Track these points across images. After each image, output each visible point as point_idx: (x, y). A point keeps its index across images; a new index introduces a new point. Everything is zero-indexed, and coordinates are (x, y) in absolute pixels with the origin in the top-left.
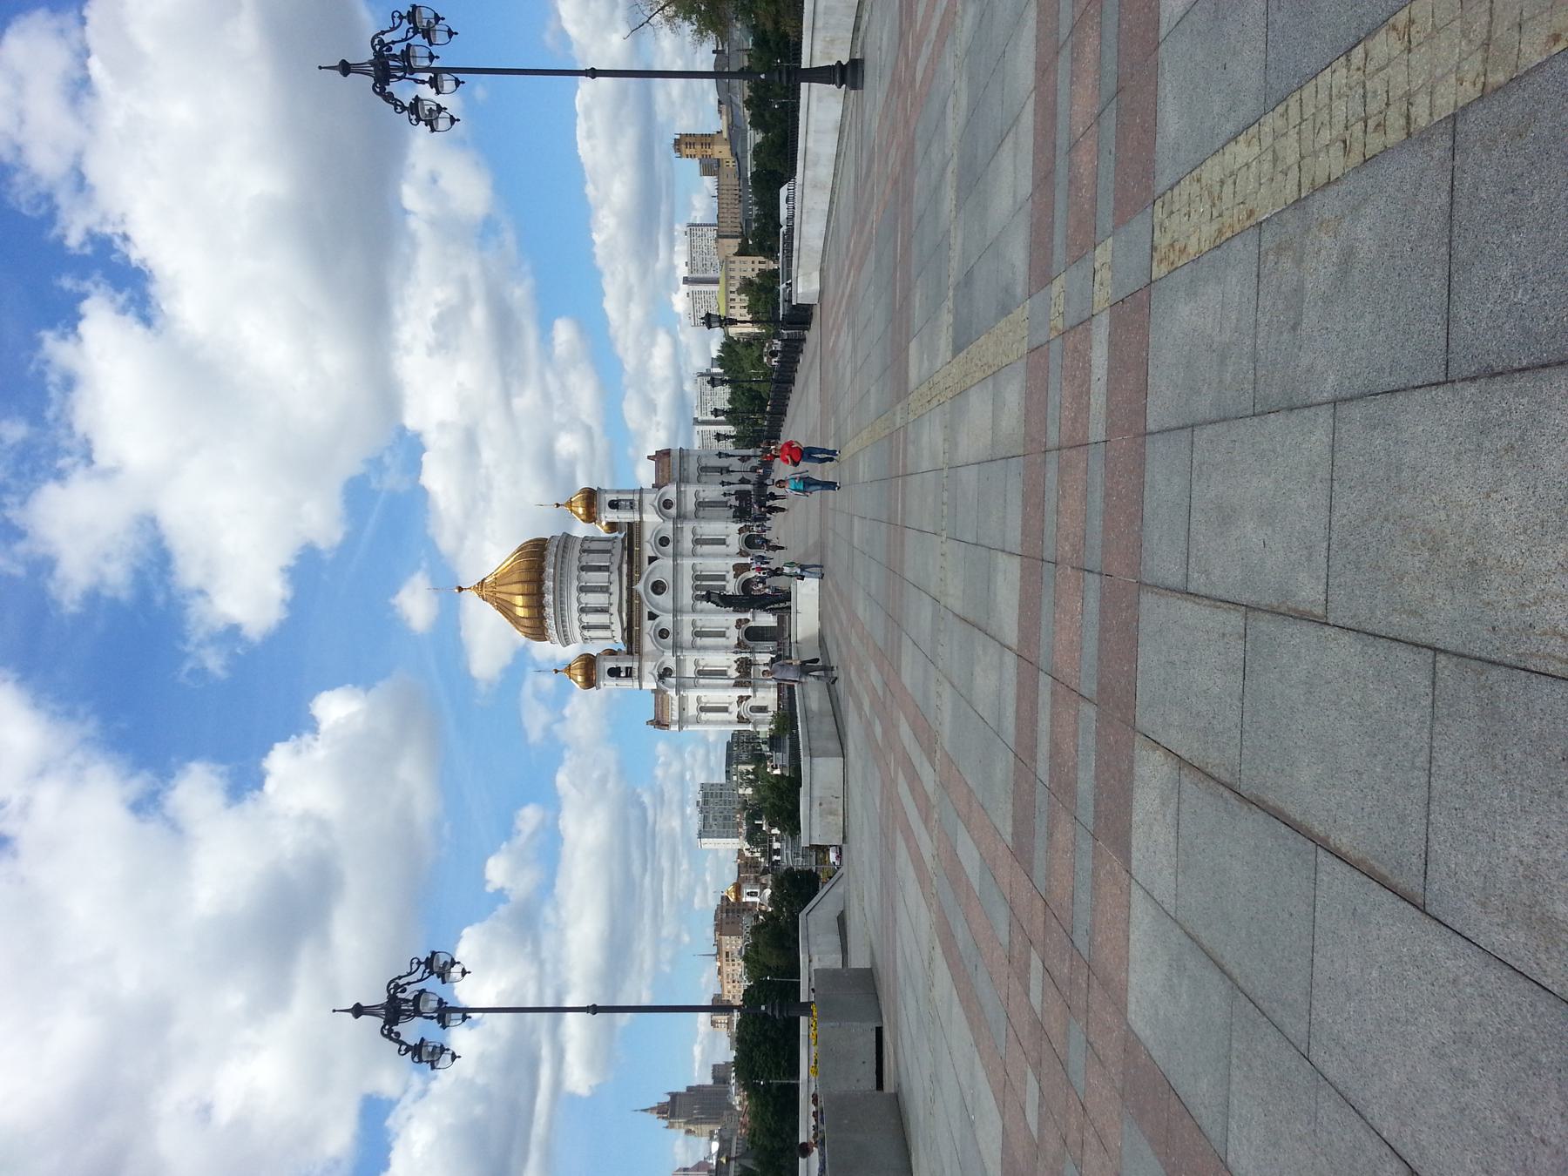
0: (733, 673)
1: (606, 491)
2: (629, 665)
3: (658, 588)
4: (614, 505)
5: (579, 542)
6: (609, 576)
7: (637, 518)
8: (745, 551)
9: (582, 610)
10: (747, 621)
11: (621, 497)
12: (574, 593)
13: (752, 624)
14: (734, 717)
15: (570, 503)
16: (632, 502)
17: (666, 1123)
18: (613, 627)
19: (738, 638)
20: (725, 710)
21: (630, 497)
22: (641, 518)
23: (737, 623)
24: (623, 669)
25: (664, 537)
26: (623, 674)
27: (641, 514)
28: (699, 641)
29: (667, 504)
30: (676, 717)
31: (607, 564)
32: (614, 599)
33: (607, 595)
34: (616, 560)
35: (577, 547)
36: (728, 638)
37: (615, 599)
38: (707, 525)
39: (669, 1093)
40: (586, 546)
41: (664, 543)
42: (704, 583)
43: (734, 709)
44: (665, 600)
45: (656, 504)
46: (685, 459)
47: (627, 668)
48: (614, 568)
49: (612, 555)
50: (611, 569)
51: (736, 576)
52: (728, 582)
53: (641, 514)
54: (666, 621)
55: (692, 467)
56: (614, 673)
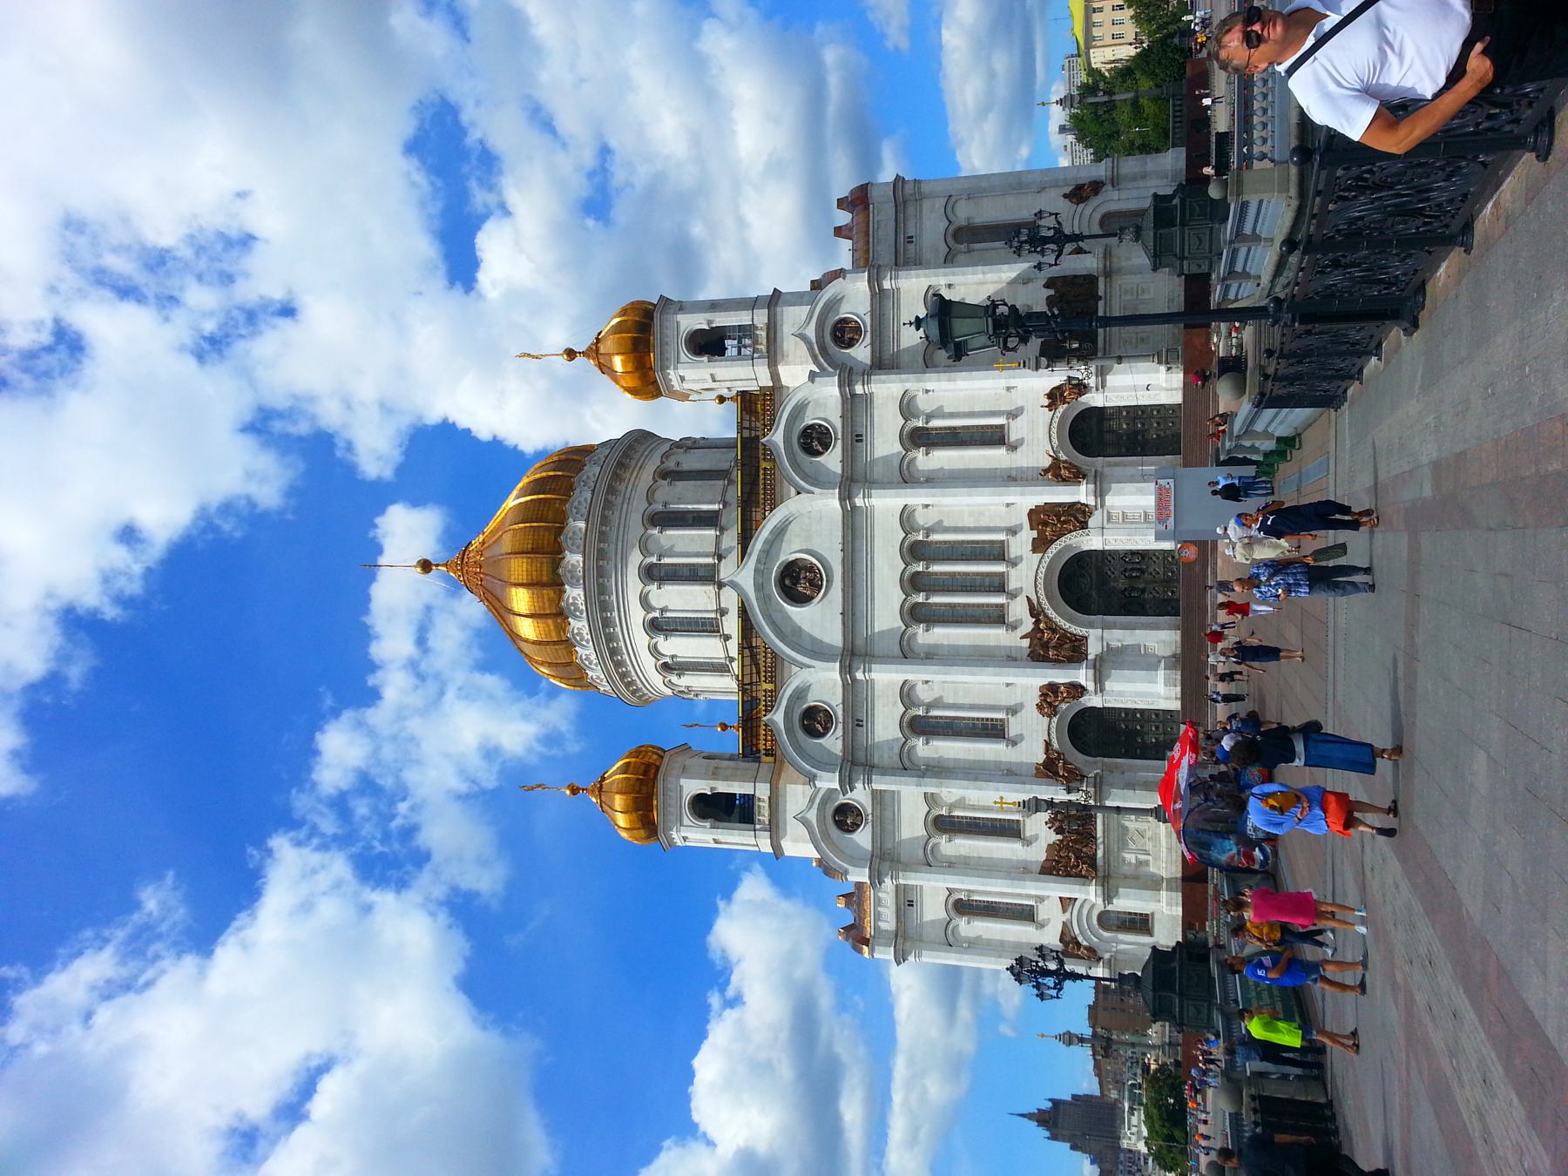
0: (1041, 833)
1: (682, 307)
4: (709, 344)
5: (666, 447)
6: (718, 539)
7: (766, 381)
8: (1070, 466)
9: (656, 626)
10: (1077, 690)
12: (634, 585)
13: (1093, 701)
15: (594, 352)
16: (745, 332)
17: (1047, 1134)
19: (1048, 744)
21: (741, 318)
22: (775, 376)
23: (1044, 695)
25: (812, 427)
27: (773, 365)
28: (925, 749)
29: (844, 333)
30: (888, 923)
31: (715, 507)
33: (710, 589)
36: (1014, 743)
39: (1050, 1100)
40: (670, 465)
42: (937, 568)
45: (811, 332)
46: (911, 210)
50: (724, 520)
51: (1040, 545)
52: (1014, 563)
53: (773, 365)
55: (931, 227)
56: (714, 808)
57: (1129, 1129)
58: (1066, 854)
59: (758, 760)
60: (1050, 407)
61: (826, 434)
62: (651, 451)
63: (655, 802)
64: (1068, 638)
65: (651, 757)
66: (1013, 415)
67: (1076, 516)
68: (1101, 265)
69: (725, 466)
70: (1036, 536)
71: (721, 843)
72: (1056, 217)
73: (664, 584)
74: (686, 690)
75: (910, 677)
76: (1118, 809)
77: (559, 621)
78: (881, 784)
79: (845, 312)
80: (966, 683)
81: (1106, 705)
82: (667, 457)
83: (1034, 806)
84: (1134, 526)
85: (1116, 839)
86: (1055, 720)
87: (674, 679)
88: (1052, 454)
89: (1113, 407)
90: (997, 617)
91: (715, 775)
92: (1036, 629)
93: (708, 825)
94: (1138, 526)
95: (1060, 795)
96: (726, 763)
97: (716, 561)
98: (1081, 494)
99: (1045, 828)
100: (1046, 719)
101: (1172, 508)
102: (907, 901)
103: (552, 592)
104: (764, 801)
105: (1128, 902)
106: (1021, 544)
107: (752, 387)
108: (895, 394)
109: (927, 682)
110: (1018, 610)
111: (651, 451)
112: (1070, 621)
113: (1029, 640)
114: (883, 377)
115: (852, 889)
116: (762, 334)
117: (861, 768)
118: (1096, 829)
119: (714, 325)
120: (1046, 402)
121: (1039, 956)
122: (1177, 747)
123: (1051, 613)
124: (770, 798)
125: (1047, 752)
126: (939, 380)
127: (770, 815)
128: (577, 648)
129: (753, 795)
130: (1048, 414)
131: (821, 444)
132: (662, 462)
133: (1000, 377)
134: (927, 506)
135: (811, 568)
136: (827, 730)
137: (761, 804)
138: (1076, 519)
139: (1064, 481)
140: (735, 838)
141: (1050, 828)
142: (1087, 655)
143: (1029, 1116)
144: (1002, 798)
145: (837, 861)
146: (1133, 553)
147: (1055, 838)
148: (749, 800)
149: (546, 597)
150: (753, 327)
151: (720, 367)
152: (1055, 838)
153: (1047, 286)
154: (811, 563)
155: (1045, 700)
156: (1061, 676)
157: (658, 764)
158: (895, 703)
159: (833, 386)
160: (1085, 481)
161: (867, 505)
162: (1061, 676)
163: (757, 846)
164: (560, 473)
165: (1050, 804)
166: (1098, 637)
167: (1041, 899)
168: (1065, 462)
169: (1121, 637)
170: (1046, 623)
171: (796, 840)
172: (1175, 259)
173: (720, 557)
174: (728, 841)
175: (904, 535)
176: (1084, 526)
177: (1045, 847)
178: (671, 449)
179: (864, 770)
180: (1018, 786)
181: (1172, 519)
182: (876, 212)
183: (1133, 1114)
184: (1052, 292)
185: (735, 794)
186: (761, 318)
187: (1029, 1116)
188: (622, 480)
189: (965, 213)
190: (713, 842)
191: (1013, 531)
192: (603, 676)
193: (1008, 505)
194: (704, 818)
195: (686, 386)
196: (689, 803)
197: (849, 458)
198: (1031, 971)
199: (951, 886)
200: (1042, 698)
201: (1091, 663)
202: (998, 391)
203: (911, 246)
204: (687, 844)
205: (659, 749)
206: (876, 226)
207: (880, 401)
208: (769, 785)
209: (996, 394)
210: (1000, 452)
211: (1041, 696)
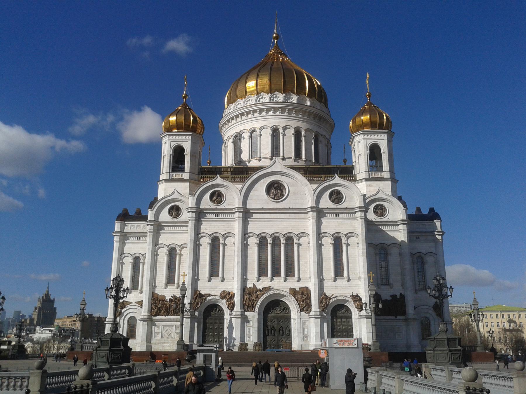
5: (328, 137)
6: (291, 158)
10: (231, 307)
11: (385, 158)
19: (209, 295)
27: (367, 179)
28: (205, 242)
33: (270, 155)
35: (322, 131)
38: (361, 251)
39: (54, 299)
40: (321, 138)
41: (334, 197)
45: (379, 196)
47: (184, 168)
51: (294, 292)
57: (44, 330)
58: (161, 303)
59: (199, 174)
60: (353, 297)
61: (339, 201)
62: (326, 131)
63: (180, 131)
64: (254, 303)
65: (200, 129)
66: (349, 280)
67: (306, 307)
68: (410, 317)
69: (321, 161)
70: (297, 290)
71: (164, 158)
72: (450, 296)
73: (271, 136)
74: (226, 145)
75: (236, 237)
76: (182, 325)
77: (255, 92)
78: (191, 225)
80: (234, 261)
81: (225, 320)
82: (323, 137)
83: (183, 289)
84: (302, 332)
85: (167, 324)
86: (219, 298)
87: (231, 140)
88: (332, 297)
89: (352, 323)
90: (262, 272)
91: (192, 156)
93: (171, 153)
94: (302, 333)
95: (187, 301)
96: (197, 160)
97: (281, 157)
98: (315, 308)
99: (172, 294)
100: (219, 294)
101: (344, 346)
102: (140, 236)
103: (267, 89)
104: (182, 176)
105: (141, 329)
106: (293, 283)
107: (355, 172)
108: (356, 230)
109: (234, 244)
110: (265, 282)
111: (326, 131)
113: (253, 287)
114: (364, 225)
115: (143, 214)
116: (379, 175)
117: (198, 216)
118: (171, 316)
119: (382, 155)
120: (354, 294)
121: (124, 289)
123: (264, 296)
124: (183, 179)
125: (206, 295)
126: (363, 249)
127: (176, 179)
128: (244, 99)
129: (184, 172)
130: (349, 295)
131: (335, 199)
132: (322, 135)
133: (365, 275)
134: (309, 244)
135: (282, 195)
136: (213, 202)
137: (180, 175)
138: (305, 307)
139: (321, 302)
140: (166, 164)
141: (172, 296)
142: (246, 312)
143: (48, 291)
144: (186, 275)
145: (157, 206)
146: (290, 331)
147: (168, 298)
148: (182, 170)
149: (265, 86)
150: (382, 171)
151: (365, 158)
152: (168, 298)
153: (401, 295)
154: (284, 195)
155: (227, 294)
156: (237, 300)
157: (197, 132)
159: (360, 205)
160: (321, 311)
161: (309, 218)
162: (237, 300)
163: (163, 174)
164: (317, 93)
165: (183, 296)
166: (253, 316)
167: (141, 292)
168: (329, 302)
169: (254, 326)
170: (260, 294)
171: (165, 189)
172: (433, 347)
173: (284, 159)
174: (164, 161)
175: (297, 234)
176: (302, 310)
177: (164, 294)
178: (327, 139)
179: (197, 218)
180: (191, 283)
181: (339, 346)
182: (429, 223)
183: (50, 331)
184: (398, 297)
185: (184, 165)
186: (386, 175)
188: (314, 118)
189: (430, 260)
190: (164, 154)
191: (299, 280)
192: (232, 110)
193: (310, 278)
194: (174, 151)
195: (356, 144)
196: (180, 145)
197: (331, 211)
198: (118, 285)
199: (147, 255)
200: (228, 293)
201: (243, 313)
202: (358, 274)
203: (415, 239)
204: (163, 144)
205: (203, 133)
206: (424, 224)
207: (353, 224)
208: (189, 178)
209: (357, 273)
210: (332, 274)
211: (229, 292)
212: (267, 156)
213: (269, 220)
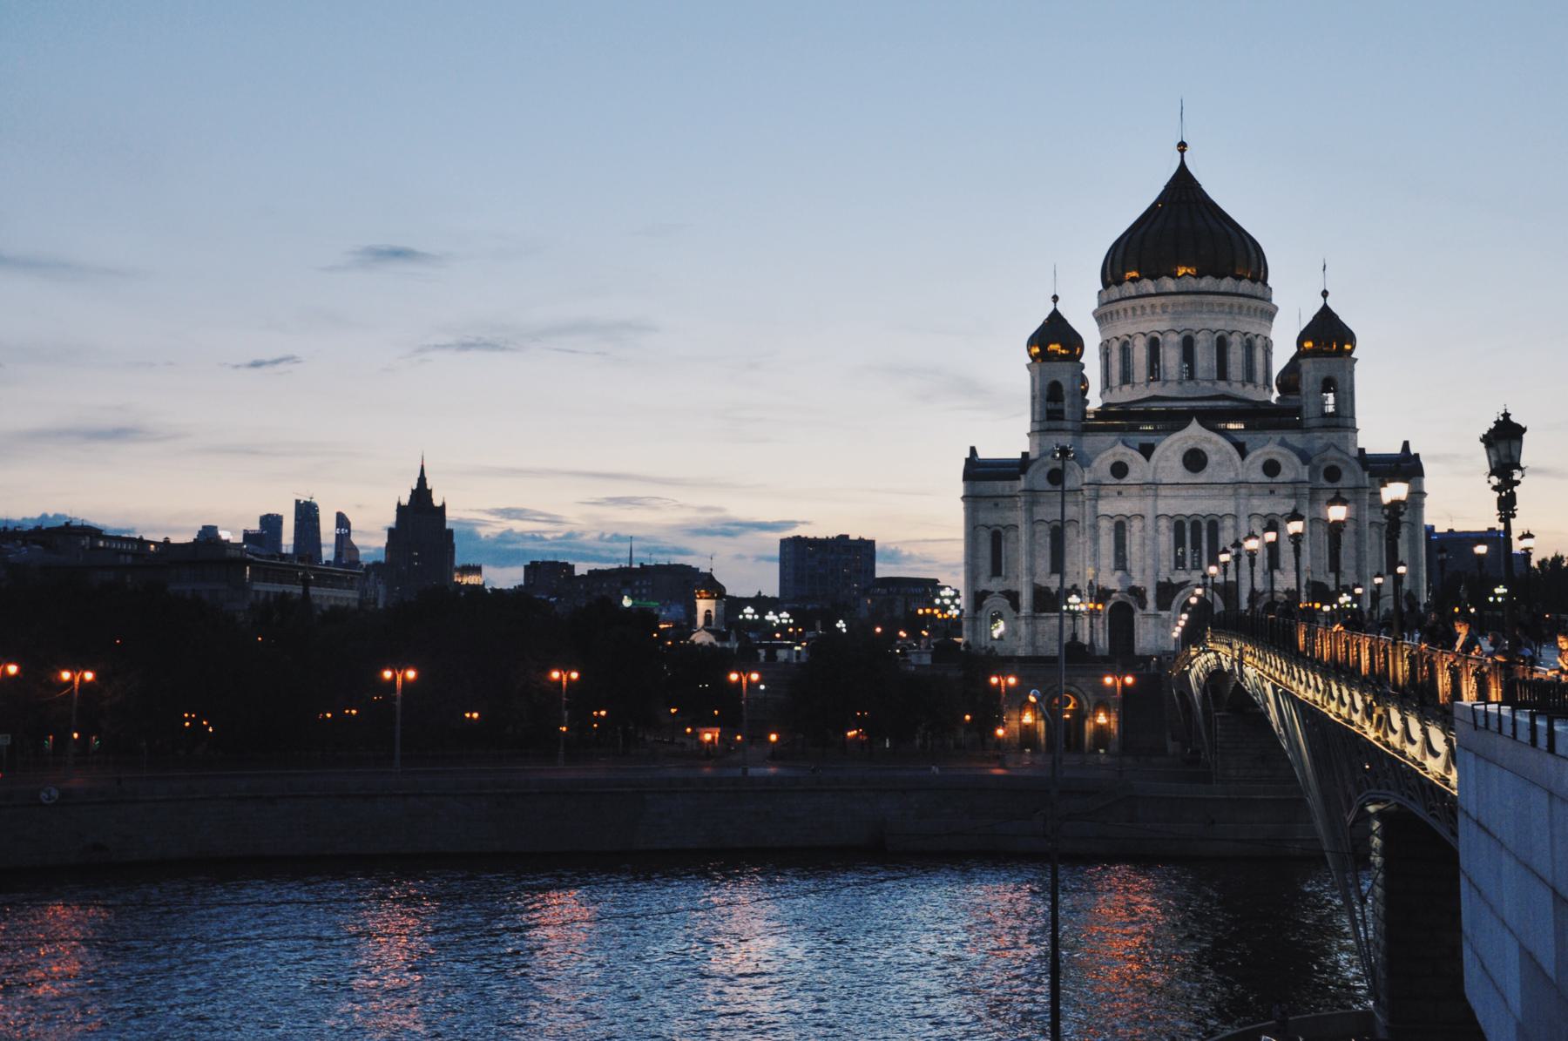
2: (1067, 410)
3: (1195, 460)
10: (1143, 607)
13: (1138, 615)
14: (984, 585)
17: (405, 501)
18: (1126, 388)
20: (996, 571)
24: (1058, 406)
26: (1051, 406)
28: (1106, 526)
32: (1170, 388)
34: (1237, 389)
35: (1254, 330)
37: (1171, 390)
40: (1259, 342)
43: (995, 585)
44: (1177, 472)
47: (1062, 411)
48: (1222, 387)
49: (1244, 385)
54: (1139, 468)
79: (1345, 474)
90: (1179, 563)
92: (1173, 585)
112: (1178, 603)
122: (1196, 649)
123: (1182, 593)
132: (1257, 336)
143: (422, 480)
156: (1150, 596)
158: (1131, 512)
162: (1150, 596)
185: (1062, 401)
187: (422, 480)
212: (1175, 378)
213: (1185, 498)
